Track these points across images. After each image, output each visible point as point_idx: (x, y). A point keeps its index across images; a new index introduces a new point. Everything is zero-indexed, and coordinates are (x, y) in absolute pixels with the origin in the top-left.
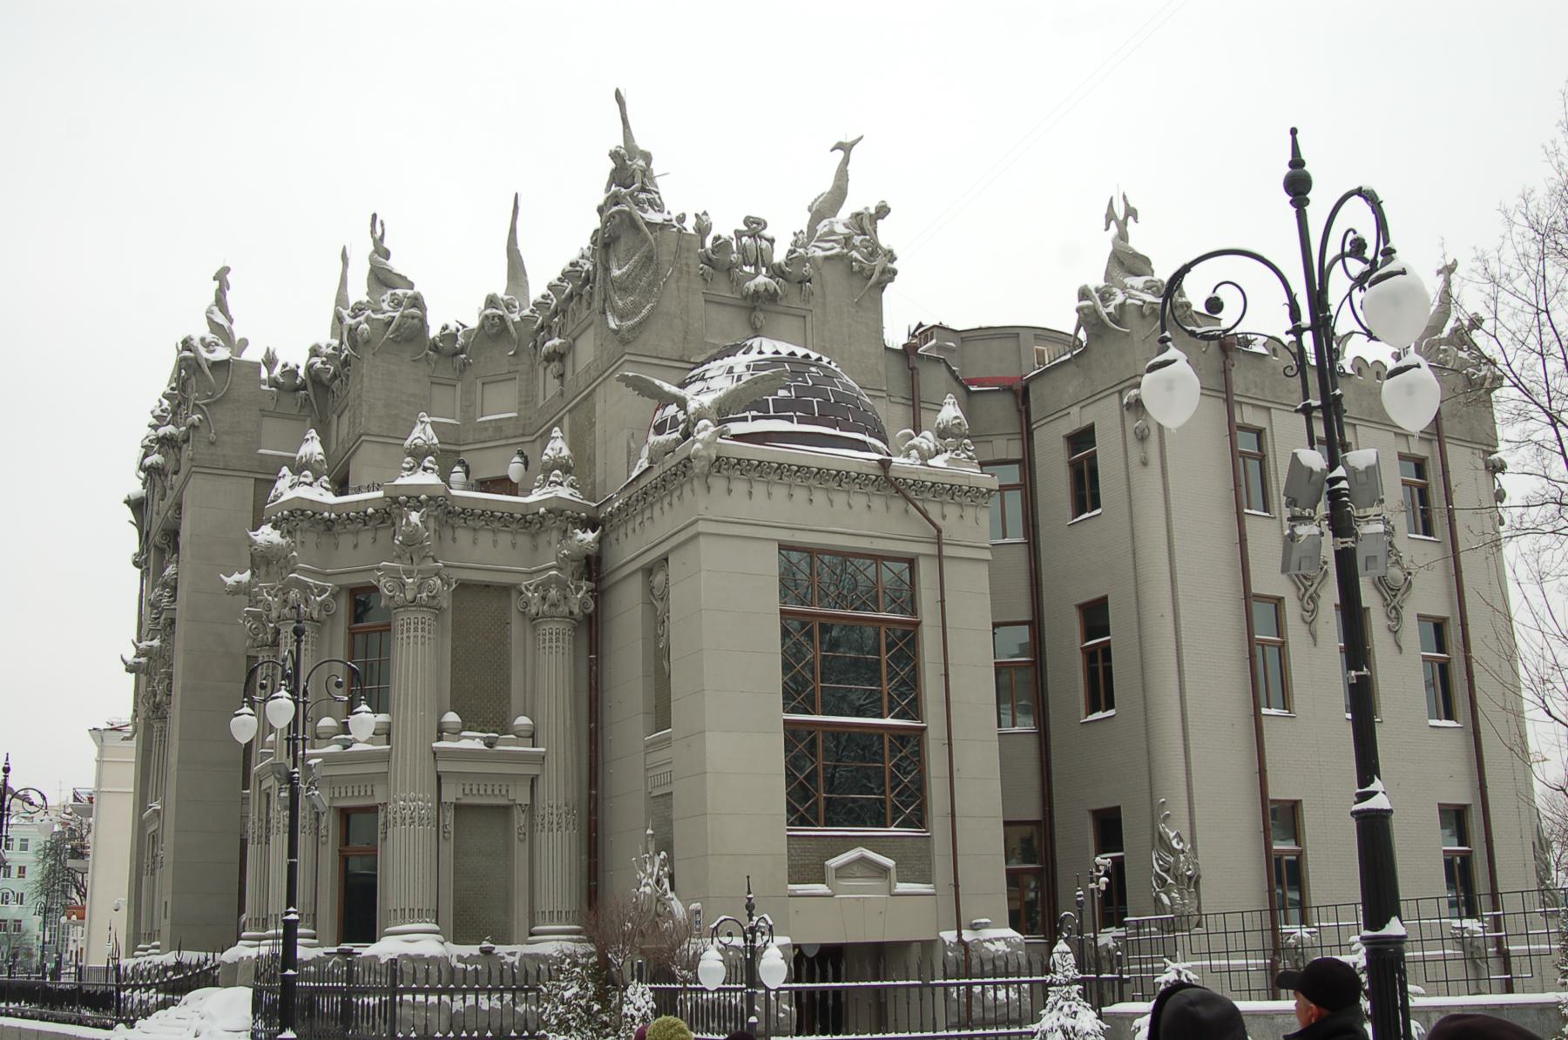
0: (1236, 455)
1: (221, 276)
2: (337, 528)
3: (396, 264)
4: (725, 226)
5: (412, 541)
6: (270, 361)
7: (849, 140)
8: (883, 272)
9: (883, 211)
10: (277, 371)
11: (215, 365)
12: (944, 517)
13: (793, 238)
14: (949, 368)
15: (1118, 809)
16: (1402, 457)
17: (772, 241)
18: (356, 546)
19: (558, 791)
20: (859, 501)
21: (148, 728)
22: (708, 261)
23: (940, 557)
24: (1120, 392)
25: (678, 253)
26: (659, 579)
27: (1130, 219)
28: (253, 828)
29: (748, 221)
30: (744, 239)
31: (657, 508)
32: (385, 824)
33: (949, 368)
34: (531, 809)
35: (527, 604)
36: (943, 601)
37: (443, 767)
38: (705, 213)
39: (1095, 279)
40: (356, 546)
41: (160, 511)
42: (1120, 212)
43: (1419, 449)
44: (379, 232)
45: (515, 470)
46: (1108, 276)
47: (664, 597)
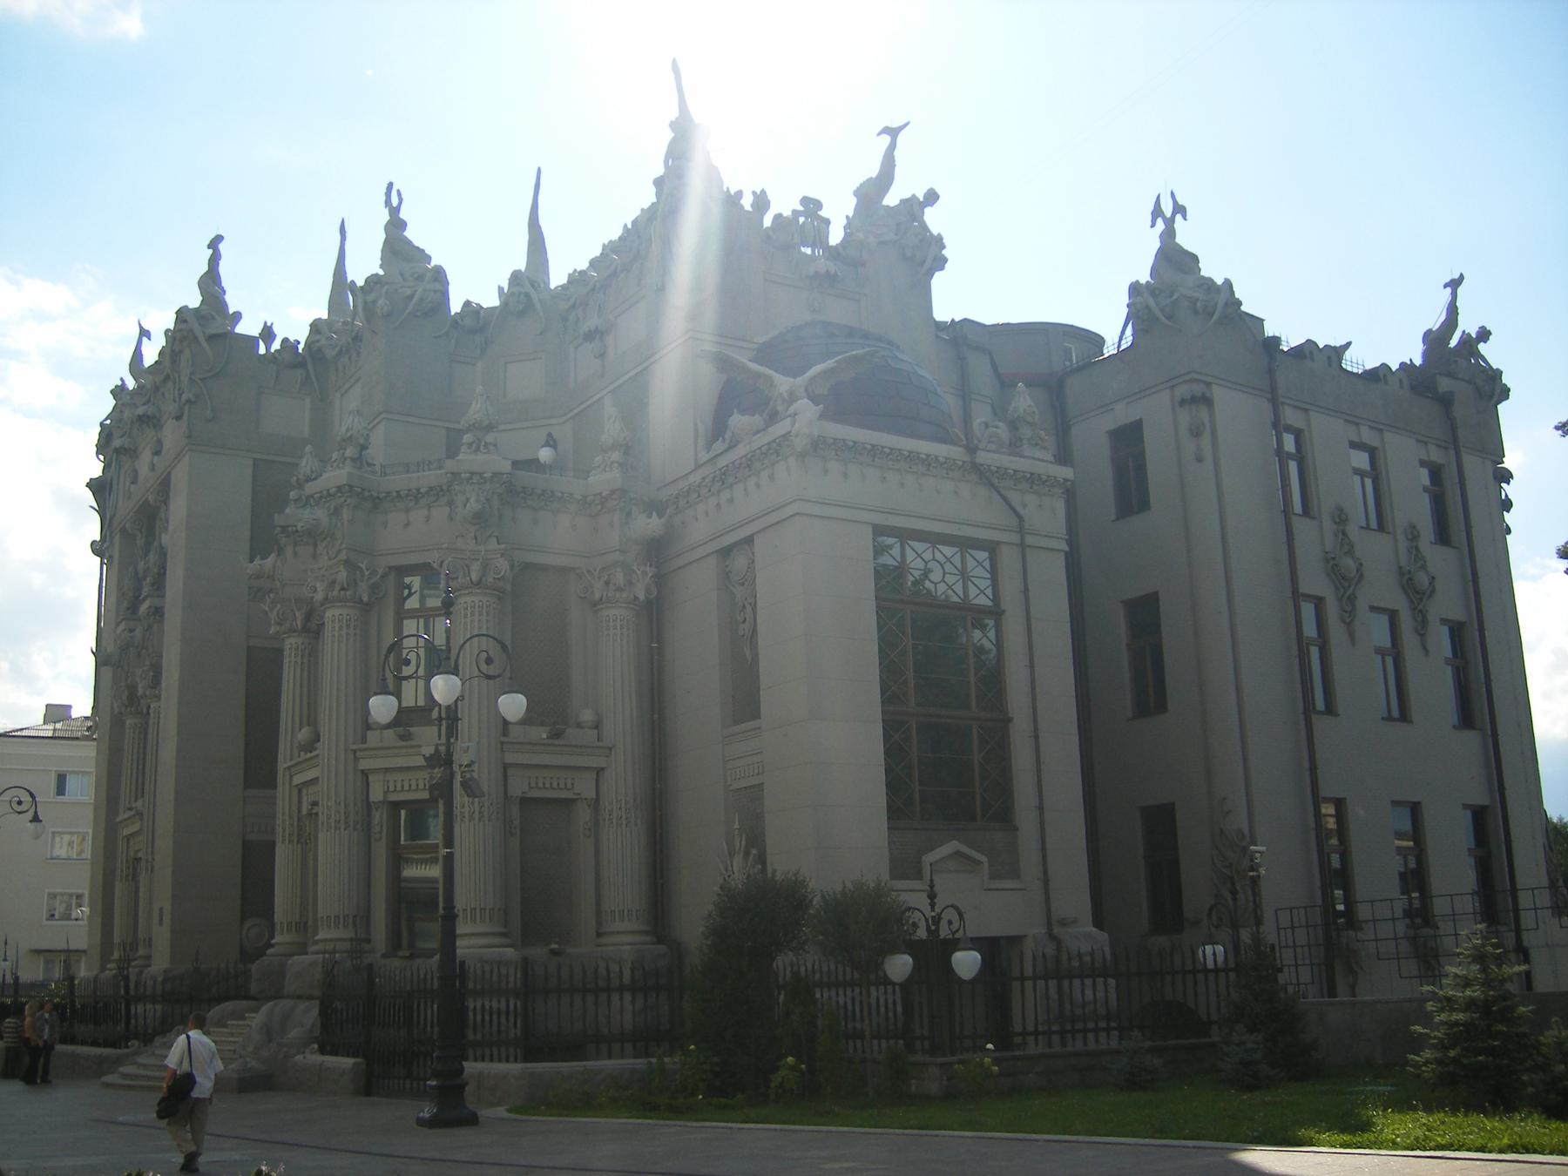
0: (1279, 450)
1: (215, 243)
3: (415, 234)
4: (784, 204)
5: (479, 518)
6: (268, 333)
7: (895, 125)
8: (935, 259)
9: (932, 197)
10: (276, 346)
11: (212, 338)
12: (1025, 506)
13: (845, 222)
14: (992, 359)
15: (1173, 805)
17: (827, 222)
18: (407, 525)
22: (767, 236)
23: (1023, 546)
24: (1172, 387)
26: (739, 562)
27: (1179, 217)
29: (806, 201)
30: (802, 220)
33: (992, 359)
34: (596, 804)
37: (511, 758)
38: (763, 192)
39: (1144, 277)
40: (407, 525)
42: (1168, 209)
43: (1436, 455)
44: (395, 202)
45: (545, 454)
46: (1154, 272)
47: (748, 580)
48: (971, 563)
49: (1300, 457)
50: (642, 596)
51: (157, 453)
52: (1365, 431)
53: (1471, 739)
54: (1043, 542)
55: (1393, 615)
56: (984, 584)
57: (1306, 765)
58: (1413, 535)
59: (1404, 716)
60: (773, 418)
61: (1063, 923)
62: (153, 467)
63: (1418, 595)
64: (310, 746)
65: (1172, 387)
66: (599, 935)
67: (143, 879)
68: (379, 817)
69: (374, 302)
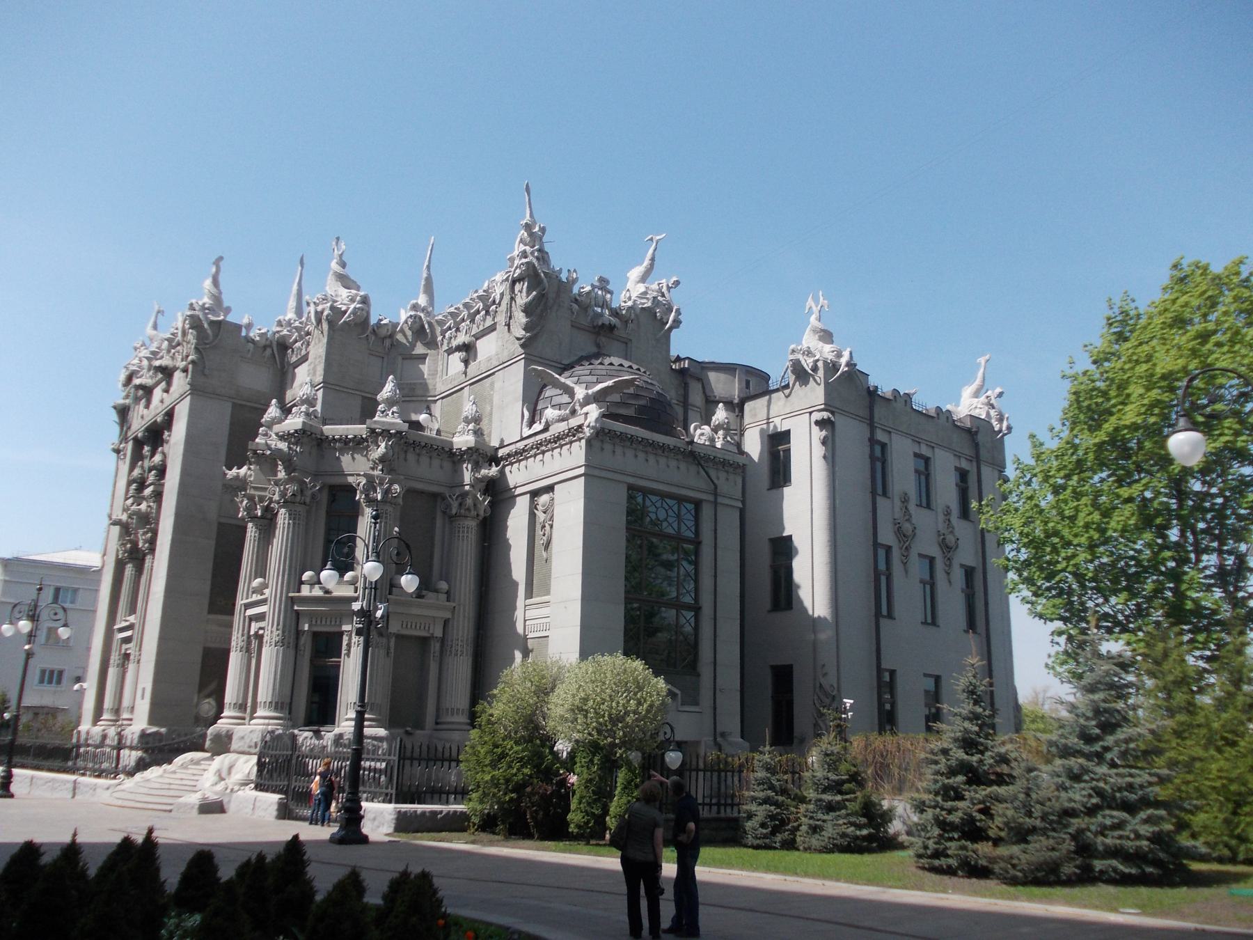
2: (325, 445)
11: (212, 323)
15: (790, 667)
16: (957, 469)
19: (463, 630)
20: (673, 463)
21: (120, 566)
23: (715, 503)
24: (811, 413)
25: (558, 293)
26: (544, 499)
28: (237, 640)
29: (602, 280)
31: (548, 455)
32: (349, 645)
34: (443, 640)
35: (449, 506)
36: (716, 530)
41: (141, 418)
43: (964, 464)
48: (683, 511)
49: (884, 463)
50: (482, 513)
51: (166, 391)
52: (924, 447)
53: (972, 641)
54: (726, 501)
55: (932, 560)
56: (691, 524)
57: (874, 648)
58: (948, 513)
59: (934, 623)
60: (573, 412)
61: (723, 735)
62: (162, 401)
63: (948, 548)
64: (259, 590)
65: (811, 413)
66: (437, 723)
67: (131, 667)
68: (306, 642)
69: (322, 312)
